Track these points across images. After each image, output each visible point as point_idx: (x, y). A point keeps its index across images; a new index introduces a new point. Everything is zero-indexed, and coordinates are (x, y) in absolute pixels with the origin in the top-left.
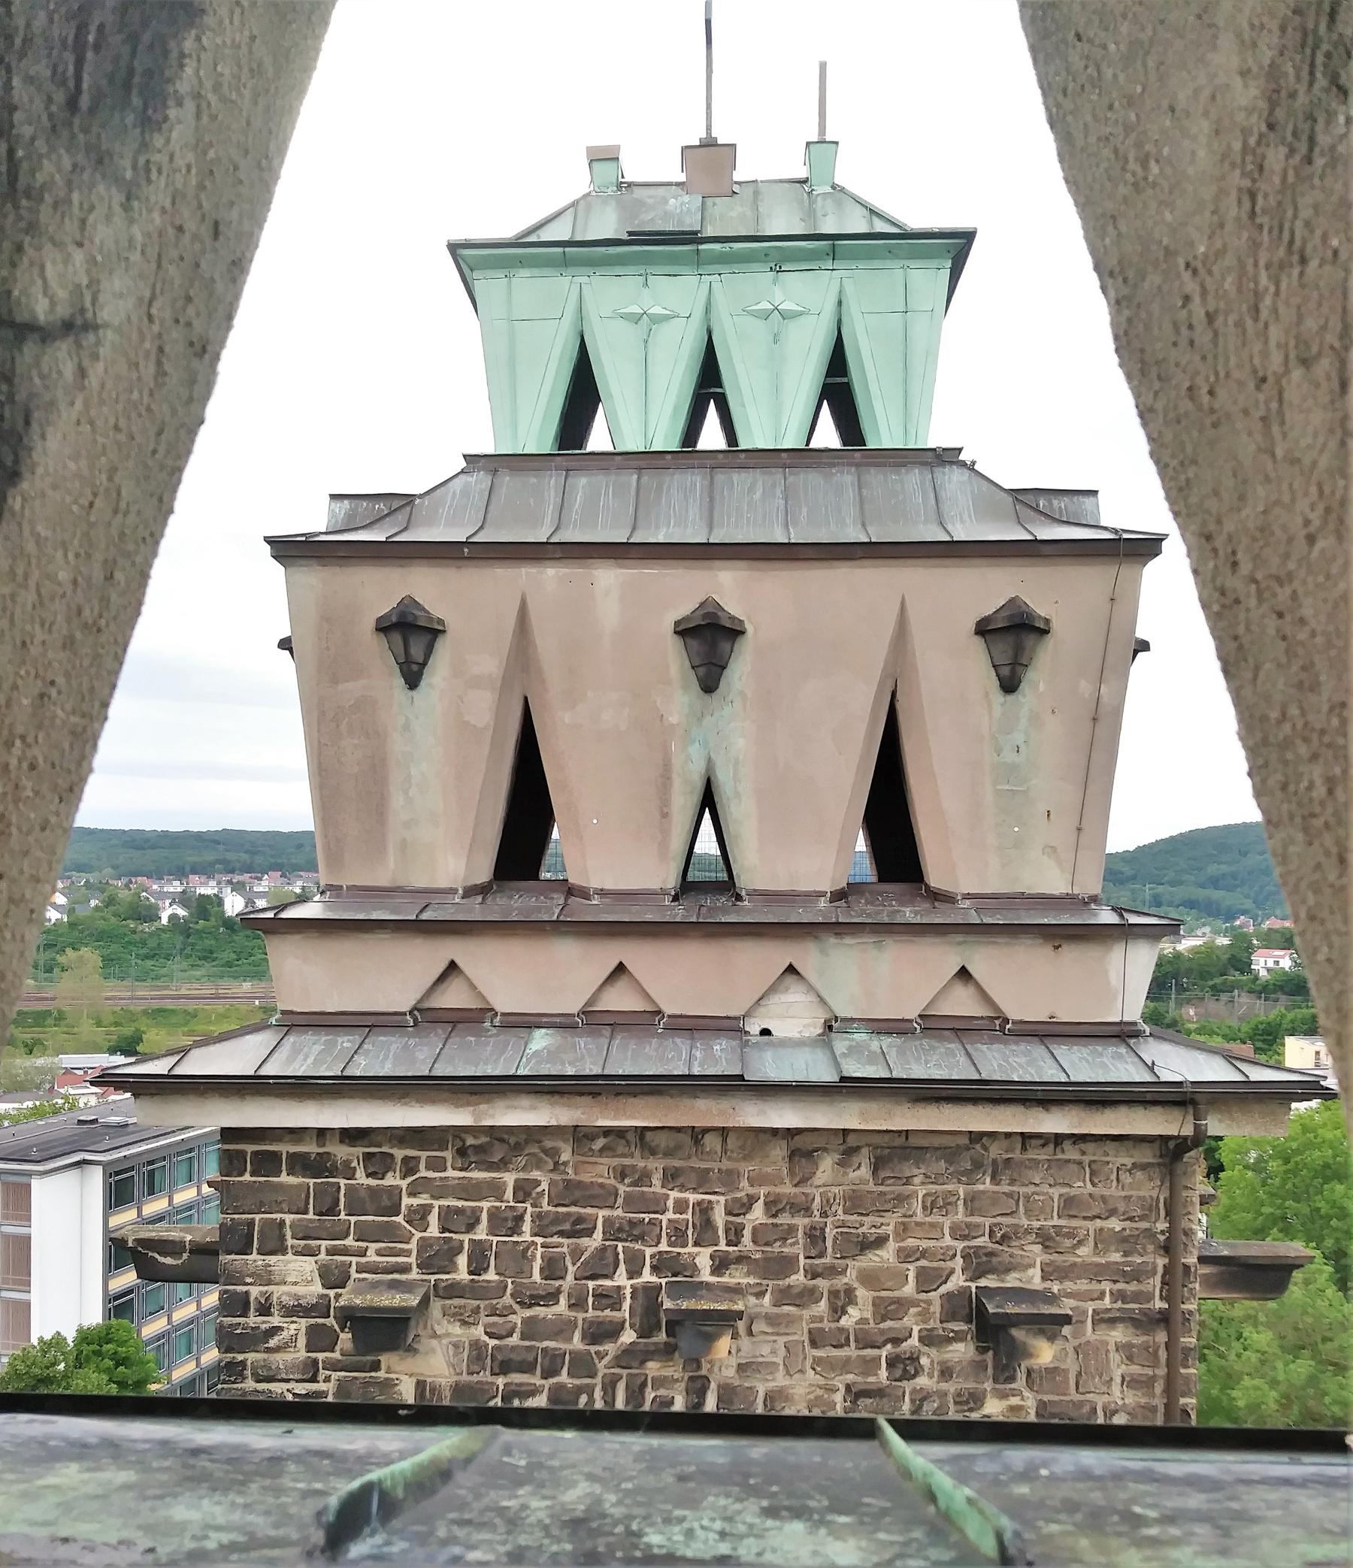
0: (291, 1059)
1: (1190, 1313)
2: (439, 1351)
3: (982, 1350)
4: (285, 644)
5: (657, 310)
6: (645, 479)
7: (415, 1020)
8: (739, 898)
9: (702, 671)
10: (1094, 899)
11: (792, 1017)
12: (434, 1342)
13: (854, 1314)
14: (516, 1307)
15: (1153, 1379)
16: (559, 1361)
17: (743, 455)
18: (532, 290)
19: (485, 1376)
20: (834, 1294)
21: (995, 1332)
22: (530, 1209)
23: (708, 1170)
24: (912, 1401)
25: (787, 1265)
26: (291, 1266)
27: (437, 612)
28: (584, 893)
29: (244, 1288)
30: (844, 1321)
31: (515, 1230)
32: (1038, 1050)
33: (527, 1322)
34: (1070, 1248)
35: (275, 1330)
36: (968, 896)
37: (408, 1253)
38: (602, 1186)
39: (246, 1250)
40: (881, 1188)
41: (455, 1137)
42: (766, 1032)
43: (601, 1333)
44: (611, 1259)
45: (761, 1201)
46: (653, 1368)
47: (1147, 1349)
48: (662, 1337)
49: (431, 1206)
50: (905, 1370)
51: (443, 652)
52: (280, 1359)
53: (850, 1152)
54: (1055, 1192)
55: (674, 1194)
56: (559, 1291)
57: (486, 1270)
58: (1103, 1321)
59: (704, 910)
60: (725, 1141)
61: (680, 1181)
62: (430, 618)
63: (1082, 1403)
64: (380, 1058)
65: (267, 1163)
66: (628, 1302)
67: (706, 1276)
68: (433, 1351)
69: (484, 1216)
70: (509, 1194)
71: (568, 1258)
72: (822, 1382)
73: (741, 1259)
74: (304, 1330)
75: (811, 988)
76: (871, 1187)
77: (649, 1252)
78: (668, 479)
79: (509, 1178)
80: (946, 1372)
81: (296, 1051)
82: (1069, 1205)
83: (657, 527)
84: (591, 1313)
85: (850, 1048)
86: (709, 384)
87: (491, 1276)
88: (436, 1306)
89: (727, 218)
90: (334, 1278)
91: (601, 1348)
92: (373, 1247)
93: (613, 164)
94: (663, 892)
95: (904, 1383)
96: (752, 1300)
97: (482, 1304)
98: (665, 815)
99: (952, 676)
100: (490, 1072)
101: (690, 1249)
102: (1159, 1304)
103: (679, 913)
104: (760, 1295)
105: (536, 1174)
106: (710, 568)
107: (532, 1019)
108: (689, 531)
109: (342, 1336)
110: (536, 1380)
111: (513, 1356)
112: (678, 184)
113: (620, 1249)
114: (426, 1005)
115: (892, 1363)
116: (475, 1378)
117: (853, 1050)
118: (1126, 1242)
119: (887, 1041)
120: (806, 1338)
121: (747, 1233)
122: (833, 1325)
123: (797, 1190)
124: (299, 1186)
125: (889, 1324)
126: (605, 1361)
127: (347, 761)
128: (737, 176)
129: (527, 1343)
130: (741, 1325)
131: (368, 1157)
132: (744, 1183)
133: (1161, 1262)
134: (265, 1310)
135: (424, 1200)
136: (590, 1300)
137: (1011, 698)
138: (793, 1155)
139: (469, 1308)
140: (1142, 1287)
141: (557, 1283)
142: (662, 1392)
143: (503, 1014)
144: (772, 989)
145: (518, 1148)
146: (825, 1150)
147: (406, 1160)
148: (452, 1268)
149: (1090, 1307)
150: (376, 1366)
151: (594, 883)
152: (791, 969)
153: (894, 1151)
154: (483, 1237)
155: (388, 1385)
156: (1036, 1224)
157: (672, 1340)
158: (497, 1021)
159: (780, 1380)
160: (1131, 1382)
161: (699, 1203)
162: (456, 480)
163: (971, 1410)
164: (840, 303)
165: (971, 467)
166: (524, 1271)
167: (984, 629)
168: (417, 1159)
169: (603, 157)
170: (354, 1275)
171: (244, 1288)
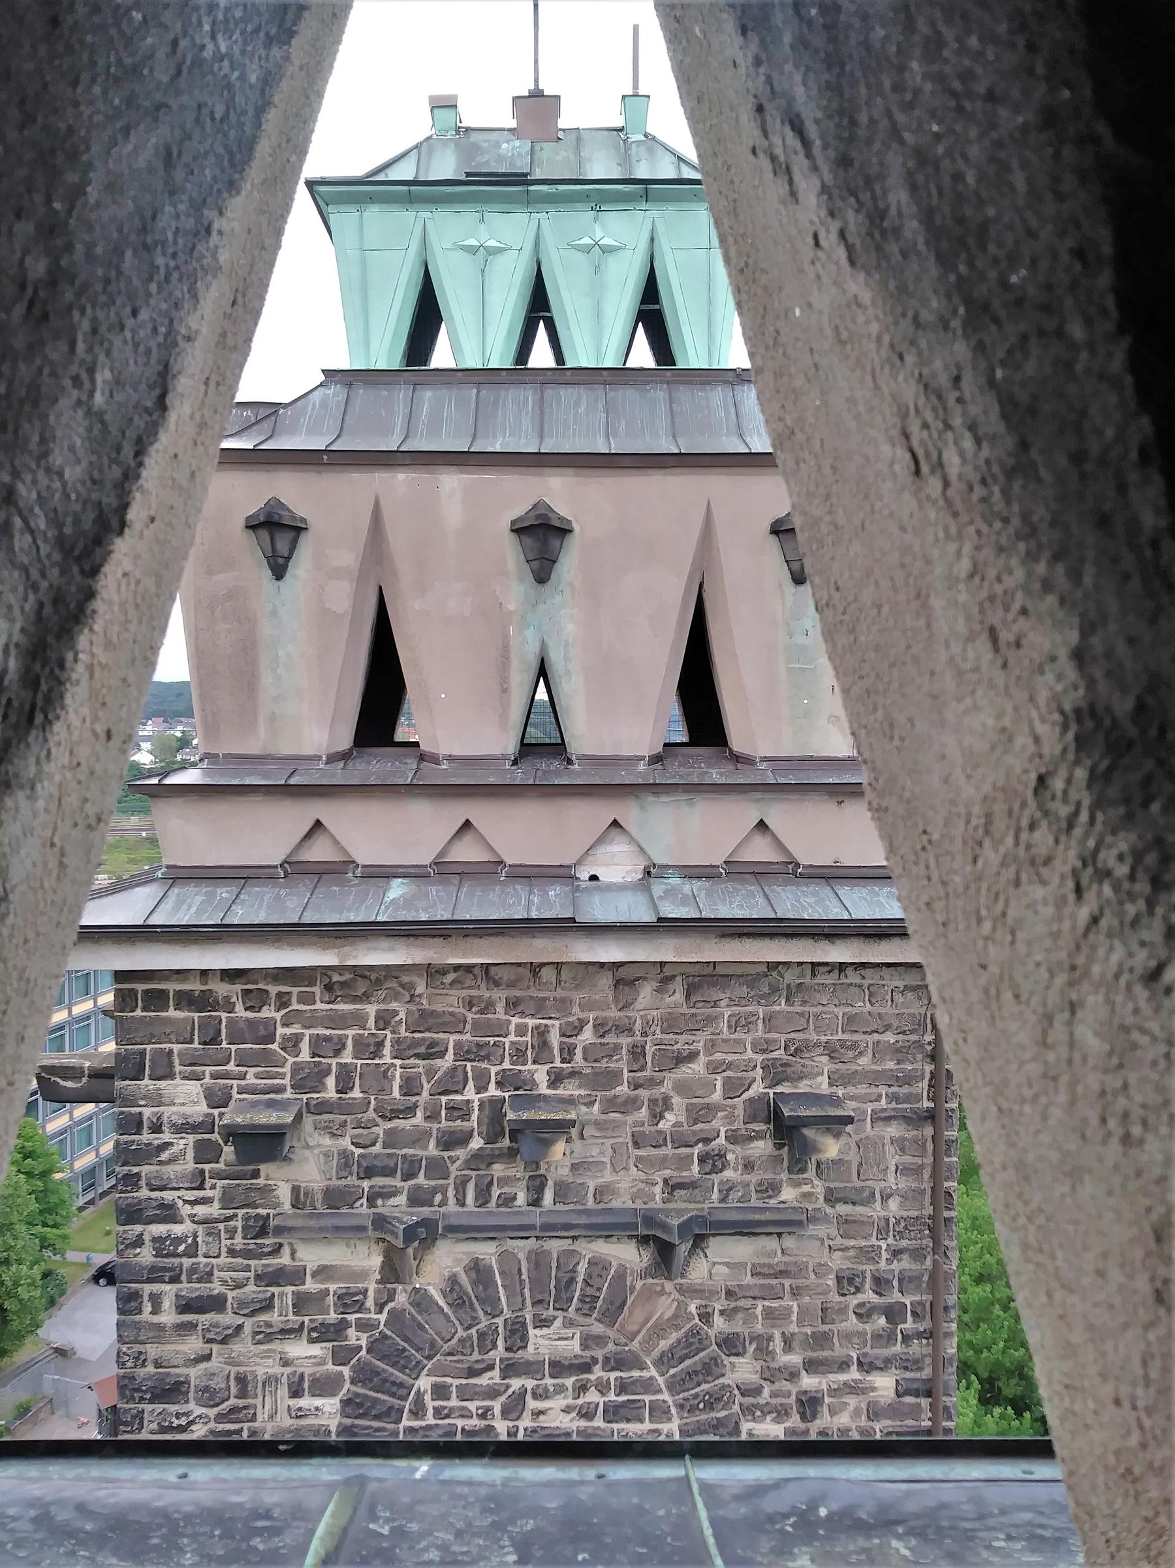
0: (176, 908)
1: (953, 1110)
3: (779, 1146)
5: (492, 243)
7: (286, 872)
8: (570, 761)
11: (617, 865)
12: (307, 1152)
13: (670, 1118)
14: (379, 1120)
17: (569, 373)
18: (379, 221)
19: (352, 1180)
20: (653, 1102)
21: (787, 1131)
22: (389, 1036)
23: (544, 999)
25: (613, 1077)
27: (300, 512)
28: (434, 759)
29: (138, 1110)
30: (661, 1125)
31: (377, 1054)
32: (825, 891)
33: (388, 1133)
35: (166, 1145)
36: (765, 759)
38: (452, 1014)
39: (138, 1076)
40: (693, 1011)
42: (594, 878)
43: (451, 1141)
46: (498, 1169)
47: (916, 1142)
48: (506, 1142)
49: (303, 1034)
52: (171, 1171)
53: (667, 980)
54: (840, 1011)
55: (515, 1020)
56: (415, 1106)
57: (352, 1089)
58: (879, 1119)
59: (540, 773)
60: (559, 973)
62: (294, 517)
64: (253, 908)
65: (156, 1000)
66: (476, 1112)
67: (543, 1089)
69: (350, 1043)
70: (371, 1023)
72: (643, 1177)
73: (573, 1074)
75: (632, 840)
76: (684, 1010)
77: (493, 1070)
78: (503, 393)
79: (371, 1010)
80: (749, 1166)
83: (495, 437)
84: (444, 1124)
85: (666, 892)
86: (538, 306)
87: (356, 1094)
88: (308, 1121)
89: (552, 163)
91: (452, 1154)
93: (449, 113)
94: (504, 758)
96: (584, 1109)
97: (349, 1118)
98: (505, 691)
100: (353, 918)
101: (530, 1066)
102: (927, 1104)
103: (518, 776)
104: (590, 1104)
105: (394, 1005)
106: (540, 474)
108: (523, 441)
109: (226, 1149)
112: (509, 130)
113: (469, 1068)
114: (295, 859)
115: (702, 1160)
116: (343, 1182)
117: (670, 893)
118: (899, 1052)
119: (697, 885)
120: (629, 1140)
121: (579, 1052)
122: (653, 1129)
123: (621, 1014)
124: (185, 1019)
125: (700, 1126)
128: (562, 123)
130: (574, 1132)
131: (246, 992)
132: (576, 1009)
133: (929, 1068)
134: (157, 1128)
135: (296, 1030)
136: (443, 1113)
138: (618, 983)
140: (913, 1090)
141: (414, 1099)
142: (506, 1190)
144: (600, 841)
145: (378, 982)
146: (645, 979)
147: (280, 995)
148: (320, 1087)
150: (256, 1174)
151: (443, 750)
152: (615, 823)
154: (349, 1060)
155: (266, 1190)
156: (824, 1039)
158: (359, 872)
159: (607, 1177)
161: (537, 1027)
162: (316, 393)
163: (770, 1197)
164: (652, 240)
166: (384, 1090)
169: (443, 105)
170: (236, 1096)
171: (138, 1110)
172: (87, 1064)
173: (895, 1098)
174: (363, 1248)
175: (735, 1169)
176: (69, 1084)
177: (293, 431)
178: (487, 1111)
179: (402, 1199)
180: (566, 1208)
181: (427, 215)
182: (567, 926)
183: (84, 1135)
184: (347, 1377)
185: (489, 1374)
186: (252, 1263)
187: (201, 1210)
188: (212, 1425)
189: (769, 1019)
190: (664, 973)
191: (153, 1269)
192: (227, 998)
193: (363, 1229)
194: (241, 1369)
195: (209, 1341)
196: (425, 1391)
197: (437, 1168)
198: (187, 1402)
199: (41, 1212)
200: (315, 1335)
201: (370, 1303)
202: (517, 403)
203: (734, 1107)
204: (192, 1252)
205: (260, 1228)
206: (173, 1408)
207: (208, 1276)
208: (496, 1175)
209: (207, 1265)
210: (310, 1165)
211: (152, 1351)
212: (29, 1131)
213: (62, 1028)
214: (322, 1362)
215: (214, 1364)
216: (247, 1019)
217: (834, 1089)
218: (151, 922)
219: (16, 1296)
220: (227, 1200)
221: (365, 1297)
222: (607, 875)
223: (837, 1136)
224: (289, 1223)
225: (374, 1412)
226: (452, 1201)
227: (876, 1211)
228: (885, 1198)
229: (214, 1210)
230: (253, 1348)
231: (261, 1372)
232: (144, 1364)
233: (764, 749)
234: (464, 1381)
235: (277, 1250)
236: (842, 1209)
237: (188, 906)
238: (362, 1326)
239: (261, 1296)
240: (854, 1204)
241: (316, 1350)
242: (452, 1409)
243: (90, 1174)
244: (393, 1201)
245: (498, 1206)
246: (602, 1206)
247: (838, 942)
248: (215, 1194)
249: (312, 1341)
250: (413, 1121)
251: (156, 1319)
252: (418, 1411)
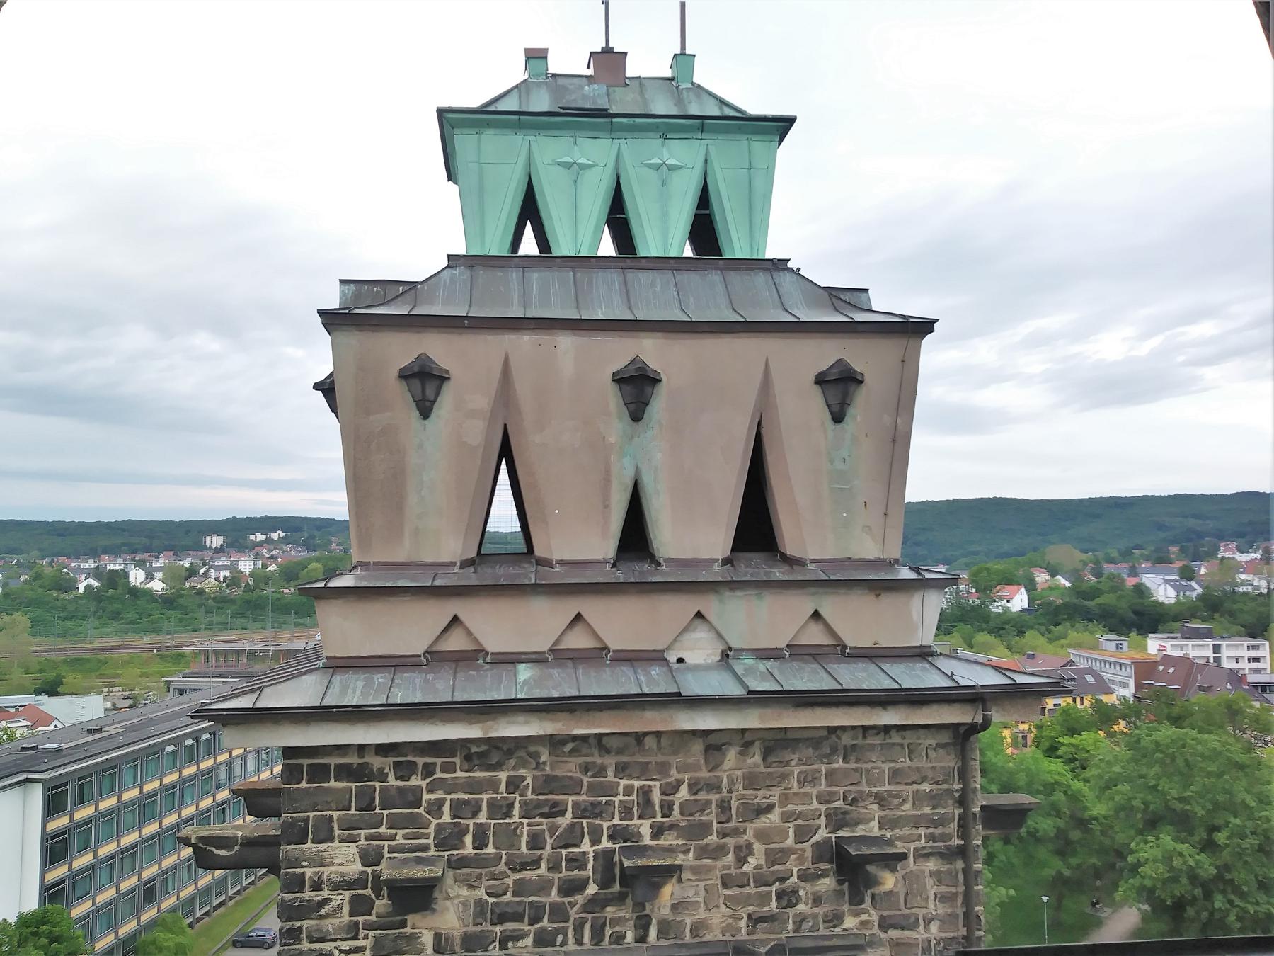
2: (452, 909)
3: (840, 882)
4: (327, 388)
5: (582, 161)
6: (579, 275)
8: (659, 564)
9: (632, 407)
10: (897, 562)
11: (699, 650)
12: (448, 903)
14: (509, 872)
15: (956, 894)
18: (494, 143)
19: (487, 926)
20: (738, 848)
21: (852, 869)
22: (518, 799)
23: (647, 763)
24: (794, 922)
25: (705, 829)
26: (337, 851)
28: (548, 563)
29: (301, 870)
30: (746, 868)
31: (508, 814)
34: (898, 805)
35: (326, 901)
37: (427, 836)
38: (571, 778)
40: (769, 770)
41: (462, 747)
42: (680, 660)
44: (579, 833)
45: (686, 784)
46: (610, 911)
48: (617, 888)
49: (445, 799)
50: (789, 901)
51: (448, 389)
53: (747, 745)
54: (886, 767)
55: (623, 782)
56: (540, 858)
57: (486, 846)
60: (659, 741)
61: (628, 772)
63: (907, 917)
64: (409, 690)
65: (319, 773)
67: (647, 841)
68: (447, 909)
70: (503, 788)
71: (547, 833)
72: (730, 912)
75: (712, 628)
76: (762, 769)
77: (605, 825)
79: (503, 776)
82: (895, 775)
84: (564, 873)
87: (490, 850)
89: (623, 102)
90: (371, 858)
92: (401, 832)
94: (605, 561)
95: (789, 910)
96: (681, 856)
97: (484, 871)
98: (606, 507)
99: (801, 409)
101: (636, 821)
103: (620, 576)
104: (686, 852)
105: (522, 772)
107: (514, 657)
109: (377, 902)
110: (525, 926)
111: (509, 910)
113: (585, 825)
114: (434, 649)
115: (779, 896)
116: (479, 928)
118: (934, 800)
120: (719, 882)
121: (676, 808)
126: (577, 907)
127: (373, 469)
131: (396, 764)
132: (673, 771)
134: (317, 886)
135: (437, 796)
136: (564, 864)
137: (839, 426)
138: (708, 749)
140: (947, 830)
141: (539, 853)
142: (617, 929)
144: (686, 630)
145: (509, 754)
146: (730, 744)
147: (426, 765)
148: (461, 845)
149: (912, 846)
150: (403, 924)
151: (556, 555)
152: (699, 615)
153: (777, 744)
155: (413, 938)
156: (874, 790)
157: (624, 890)
158: (489, 659)
159: (702, 914)
160: (940, 898)
161: (642, 787)
163: (835, 926)
165: (797, 272)
166: (514, 845)
167: (820, 380)
168: (435, 764)
170: (387, 855)
171: (301, 870)
172: (240, 834)
173: (931, 837)
175: (806, 904)
177: (431, 302)
178: (601, 861)
179: (529, 941)
180: (667, 943)
181: (532, 138)
182: (675, 700)
189: (830, 775)
190: (745, 738)
192: (381, 770)
197: (559, 913)
202: (608, 282)
203: (804, 850)
208: (609, 916)
216: (398, 788)
217: (883, 832)
218: (325, 703)
222: (690, 658)
223: (893, 870)
226: (571, 941)
227: (919, 934)
228: (928, 922)
233: (812, 554)
236: (894, 934)
237: (353, 690)
240: (903, 929)
244: (521, 943)
245: (610, 944)
246: (697, 940)
247: (889, 708)
248: (368, 943)
250: (539, 872)
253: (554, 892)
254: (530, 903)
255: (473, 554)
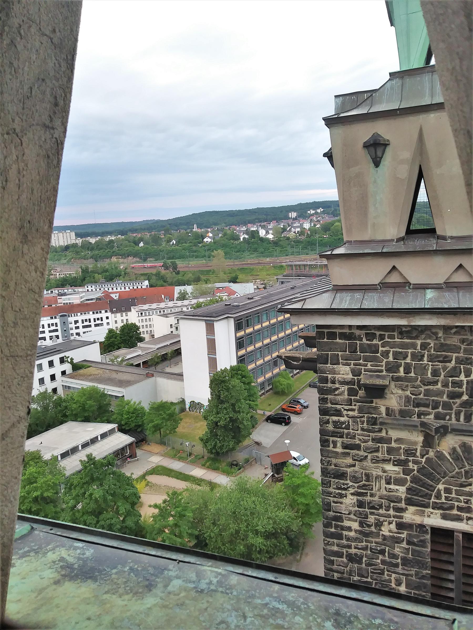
2: (394, 398)
4: (329, 155)
12: (392, 395)
14: (422, 385)
16: (438, 404)
22: (426, 353)
31: (421, 359)
35: (337, 389)
37: (382, 366)
38: (455, 345)
44: (458, 371)
56: (438, 381)
57: (411, 373)
64: (372, 301)
65: (332, 336)
68: (392, 398)
69: (409, 355)
70: (419, 347)
74: (347, 389)
79: (419, 342)
81: (341, 300)
84: (450, 389)
87: (412, 374)
90: (356, 373)
91: (454, 401)
100: (414, 306)
105: (429, 341)
109: (360, 392)
114: (383, 282)
116: (407, 408)
126: (457, 405)
129: (426, 398)
134: (333, 382)
136: (450, 384)
139: (405, 385)
141: (437, 378)
143: (413, 284)
147: (380, 335)
150: (372, 402)
151: (449, 234)
154: (409, 362)
155: (376, 408)
168: (385, 335)
170: (363, 372)
174: (415, 434)
176: (295, 363)
179: (432, 416)
183: (260, 371)
184: (409, 480)
185: (470, 487)
186: (370, 434)
187: (351, 413)
188: (356, 489)
191: (333, 432)
192: (360, 336)
193: (416, 426)
194: (367, 471)
195: (354, 460)
196: (441, 490)
197: (447, 406)
198: (347, 480)
199: (249, 396)
200: (396, 463)
201: (418, 454)
204: (348, 428)
205: (373, 422)
206: (342, 481)
207: (354, 437)
209: (353, 433)
210: (394, 400)
211: (334, 461)
212: (243, 369)
213: (251, 334)
214: (399, 473)
215: (356, 468)
219: (243, 423)
220: (361, 410)
221: (416, 452)
224: (386, 421)
225: (420, 494)
229: (356, 413)
230: (371, 464)
231: (374, 473)
232: (331, 465)
234: (458, 488)
235: (380, 431)
237: (346, 301)
238: (415, 462)
239: (374, 446)
241: (396, 468)
242: (453, 498)
243: (263, 384)
244: (427, 417)
249: (394, 465)
250: (437, 387)
251: (335, 450)
252: (438, 496)
253: (445, 397)
254: (433, 400)
255: (403, 234)
